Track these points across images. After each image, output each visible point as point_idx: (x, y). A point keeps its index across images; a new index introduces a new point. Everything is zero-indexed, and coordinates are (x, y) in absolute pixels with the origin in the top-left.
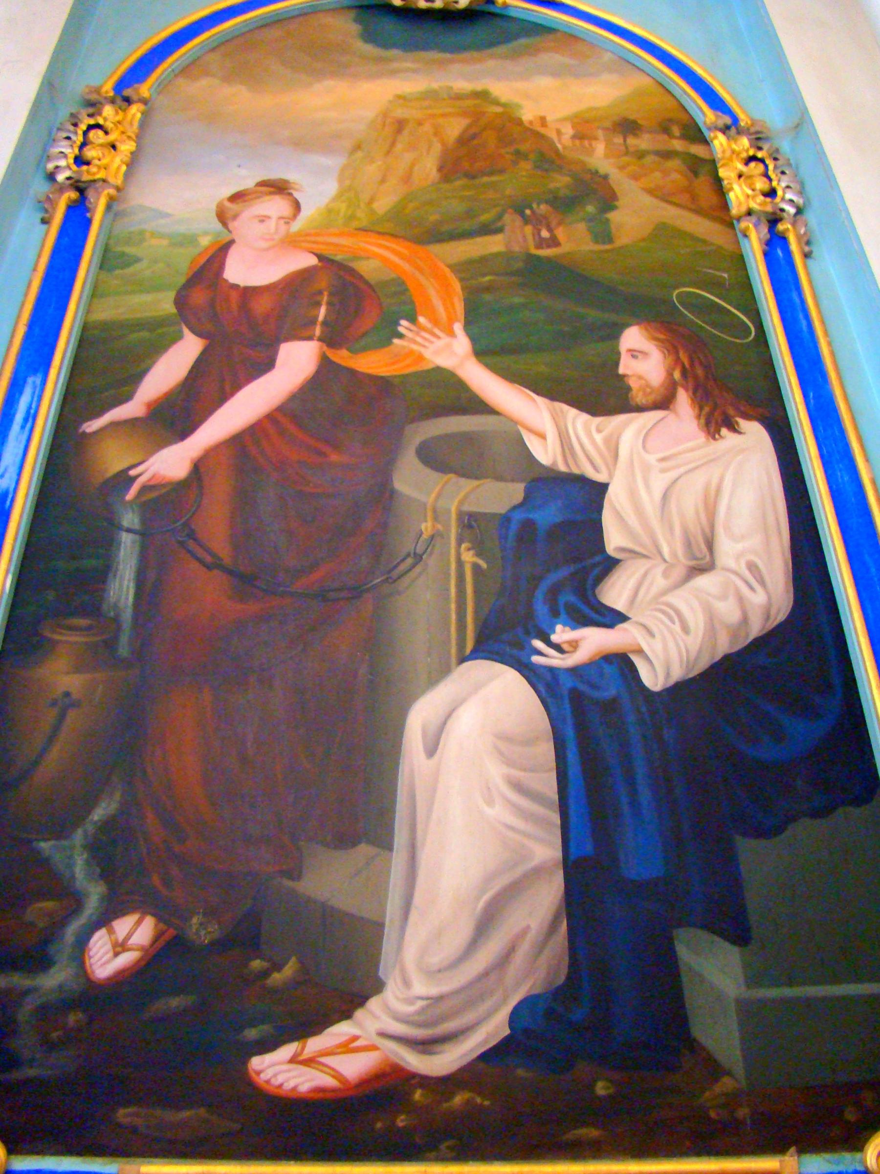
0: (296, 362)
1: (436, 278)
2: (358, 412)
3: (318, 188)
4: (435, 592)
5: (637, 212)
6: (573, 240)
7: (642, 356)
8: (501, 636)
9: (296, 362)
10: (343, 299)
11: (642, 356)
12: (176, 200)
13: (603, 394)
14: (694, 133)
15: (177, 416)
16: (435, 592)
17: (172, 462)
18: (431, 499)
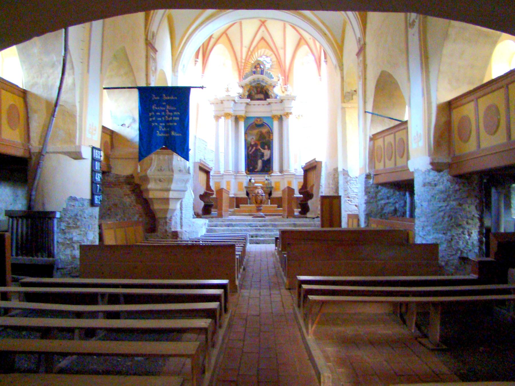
0: (254, 148)
1: (258, 143)
2: (257, 150)
3: (254, 138)
4: (259, 157)
5: (267, 138)
6: (264, 141)
7: (266, 147)
8: (261, 159)
9: (254, 148)
10: (256, 145)
11: (266, 147)
12: (249, 139)
13: (264, 149)
14: (270, 132)
15: (250, 151)
16: (259, 157)
17: (251, 153)
18: (259, 153)
